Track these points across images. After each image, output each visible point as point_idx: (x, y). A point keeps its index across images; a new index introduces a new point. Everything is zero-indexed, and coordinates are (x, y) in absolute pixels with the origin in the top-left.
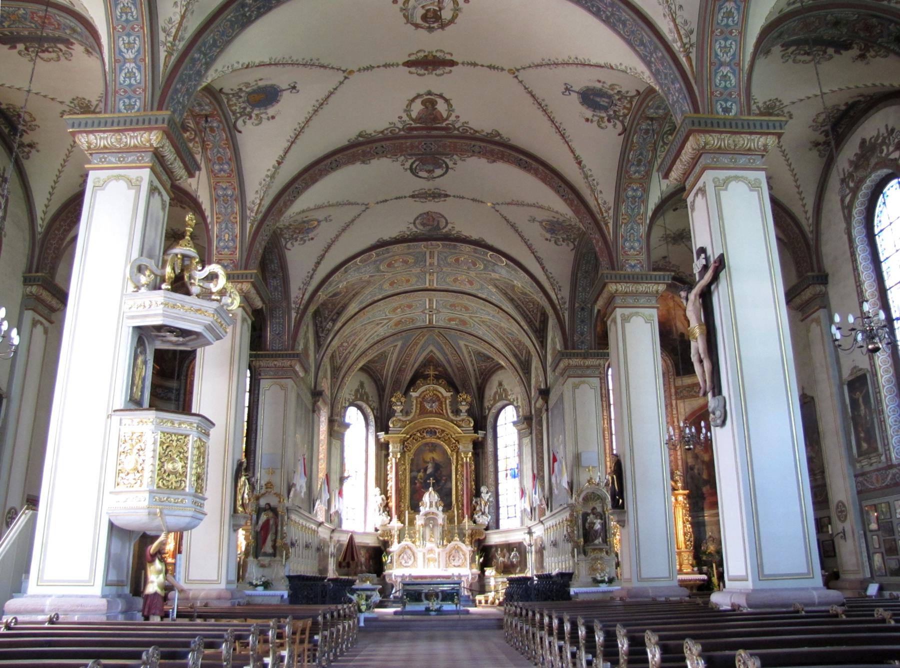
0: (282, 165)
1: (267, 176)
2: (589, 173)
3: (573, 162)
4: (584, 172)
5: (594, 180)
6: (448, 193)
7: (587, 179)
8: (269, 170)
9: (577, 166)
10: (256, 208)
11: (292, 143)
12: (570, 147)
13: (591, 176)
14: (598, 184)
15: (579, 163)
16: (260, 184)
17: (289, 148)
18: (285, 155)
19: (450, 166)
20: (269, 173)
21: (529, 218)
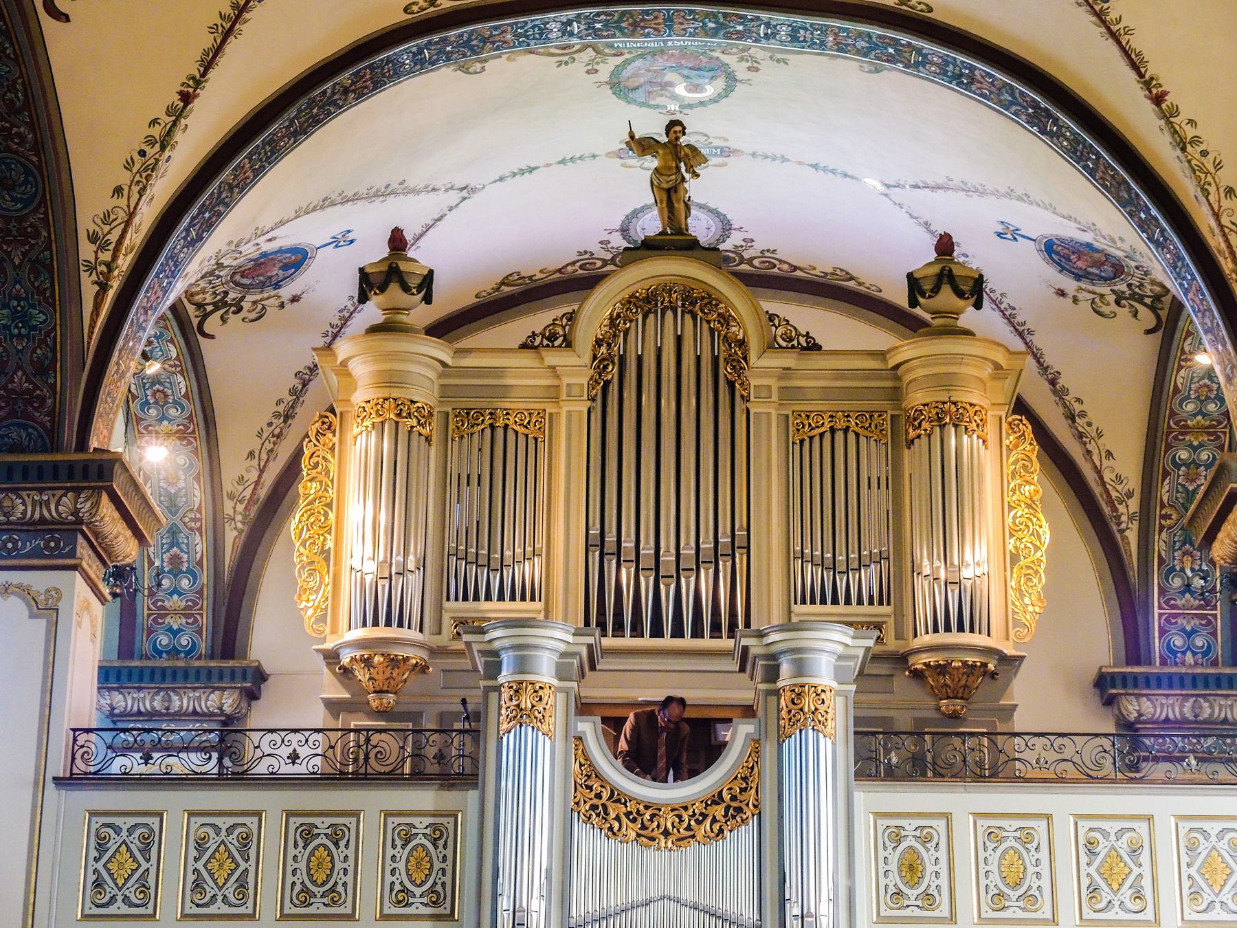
0: (196, 103)
1: (151, 141)
2: (1190, 132)
3: (1139, 93)
4: (1170, 124)
5: (1204, 153)
6: (733, 144)
7: (1183, 149)
8: (154, 122)
9: (1149, 106)
10: (113, 237)
11: (227, 34)
12: (1126, 52)
13: (1196, 140)
14: (1218, 166)
15: (1158, 100)
16: (129, 165)
17: (218, 50)
18: (204, 75)
19: (739, 76)
20: (156, 131)
21: (1000, 229)
